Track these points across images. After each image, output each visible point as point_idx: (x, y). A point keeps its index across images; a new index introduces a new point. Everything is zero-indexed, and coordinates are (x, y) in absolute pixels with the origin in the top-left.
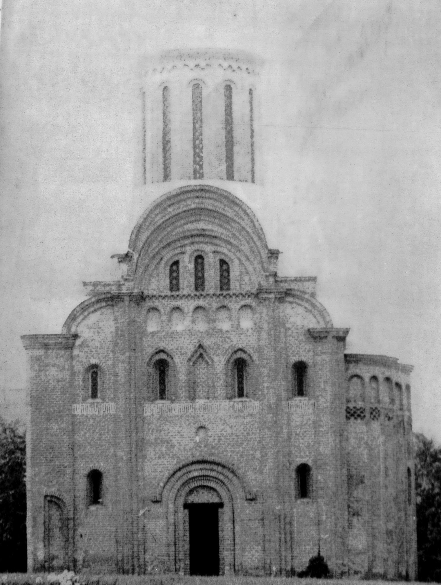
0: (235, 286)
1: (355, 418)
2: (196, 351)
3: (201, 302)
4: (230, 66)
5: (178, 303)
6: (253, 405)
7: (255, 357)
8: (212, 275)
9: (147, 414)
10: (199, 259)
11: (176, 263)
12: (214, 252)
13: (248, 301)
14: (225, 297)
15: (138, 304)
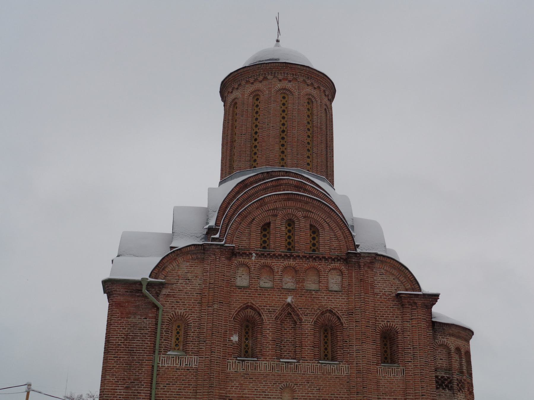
0: (323, 250)
1: (444, 389)
2: (284, 310)
3: (292, 262)
4: (312, 84)
5: (269, 261)
6: (341, 369)
7: (343, 320)
8: (303, 238)
9: (231, 370)
10: (290, 223)
11: (269, 224)
12: (305, 217)
13: (337, 265)
14: (314, 259)
15: (229, 259)
